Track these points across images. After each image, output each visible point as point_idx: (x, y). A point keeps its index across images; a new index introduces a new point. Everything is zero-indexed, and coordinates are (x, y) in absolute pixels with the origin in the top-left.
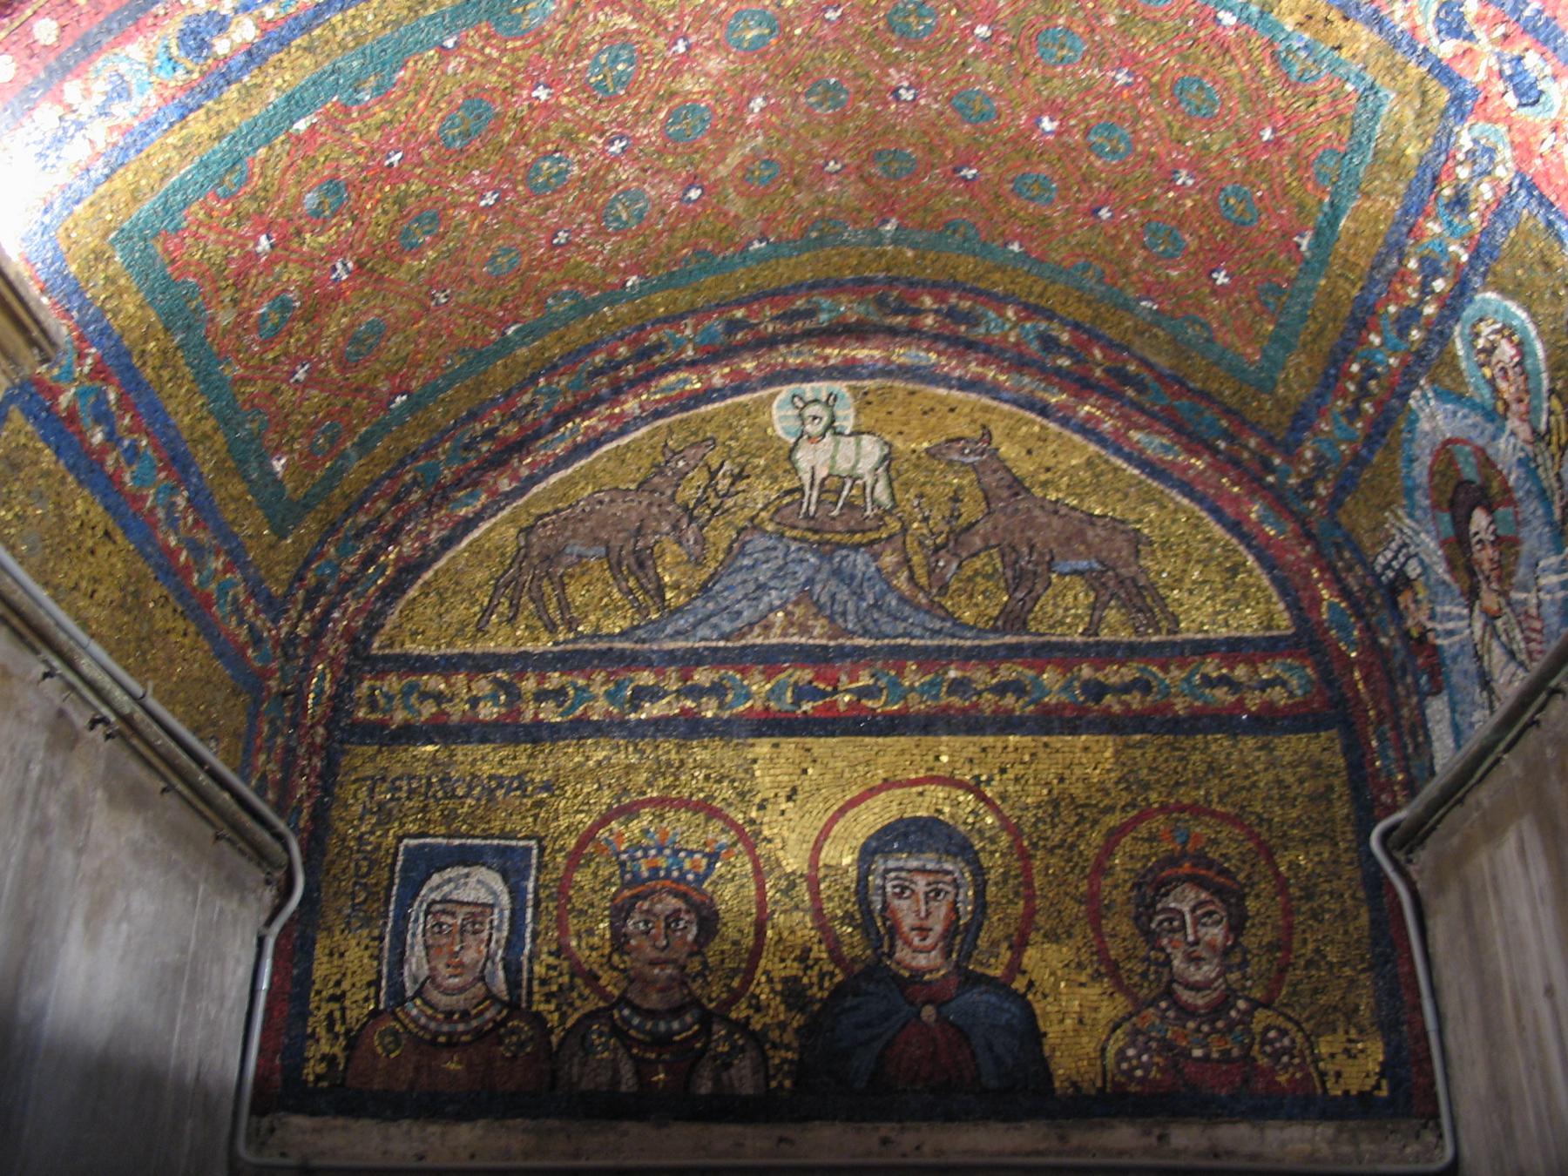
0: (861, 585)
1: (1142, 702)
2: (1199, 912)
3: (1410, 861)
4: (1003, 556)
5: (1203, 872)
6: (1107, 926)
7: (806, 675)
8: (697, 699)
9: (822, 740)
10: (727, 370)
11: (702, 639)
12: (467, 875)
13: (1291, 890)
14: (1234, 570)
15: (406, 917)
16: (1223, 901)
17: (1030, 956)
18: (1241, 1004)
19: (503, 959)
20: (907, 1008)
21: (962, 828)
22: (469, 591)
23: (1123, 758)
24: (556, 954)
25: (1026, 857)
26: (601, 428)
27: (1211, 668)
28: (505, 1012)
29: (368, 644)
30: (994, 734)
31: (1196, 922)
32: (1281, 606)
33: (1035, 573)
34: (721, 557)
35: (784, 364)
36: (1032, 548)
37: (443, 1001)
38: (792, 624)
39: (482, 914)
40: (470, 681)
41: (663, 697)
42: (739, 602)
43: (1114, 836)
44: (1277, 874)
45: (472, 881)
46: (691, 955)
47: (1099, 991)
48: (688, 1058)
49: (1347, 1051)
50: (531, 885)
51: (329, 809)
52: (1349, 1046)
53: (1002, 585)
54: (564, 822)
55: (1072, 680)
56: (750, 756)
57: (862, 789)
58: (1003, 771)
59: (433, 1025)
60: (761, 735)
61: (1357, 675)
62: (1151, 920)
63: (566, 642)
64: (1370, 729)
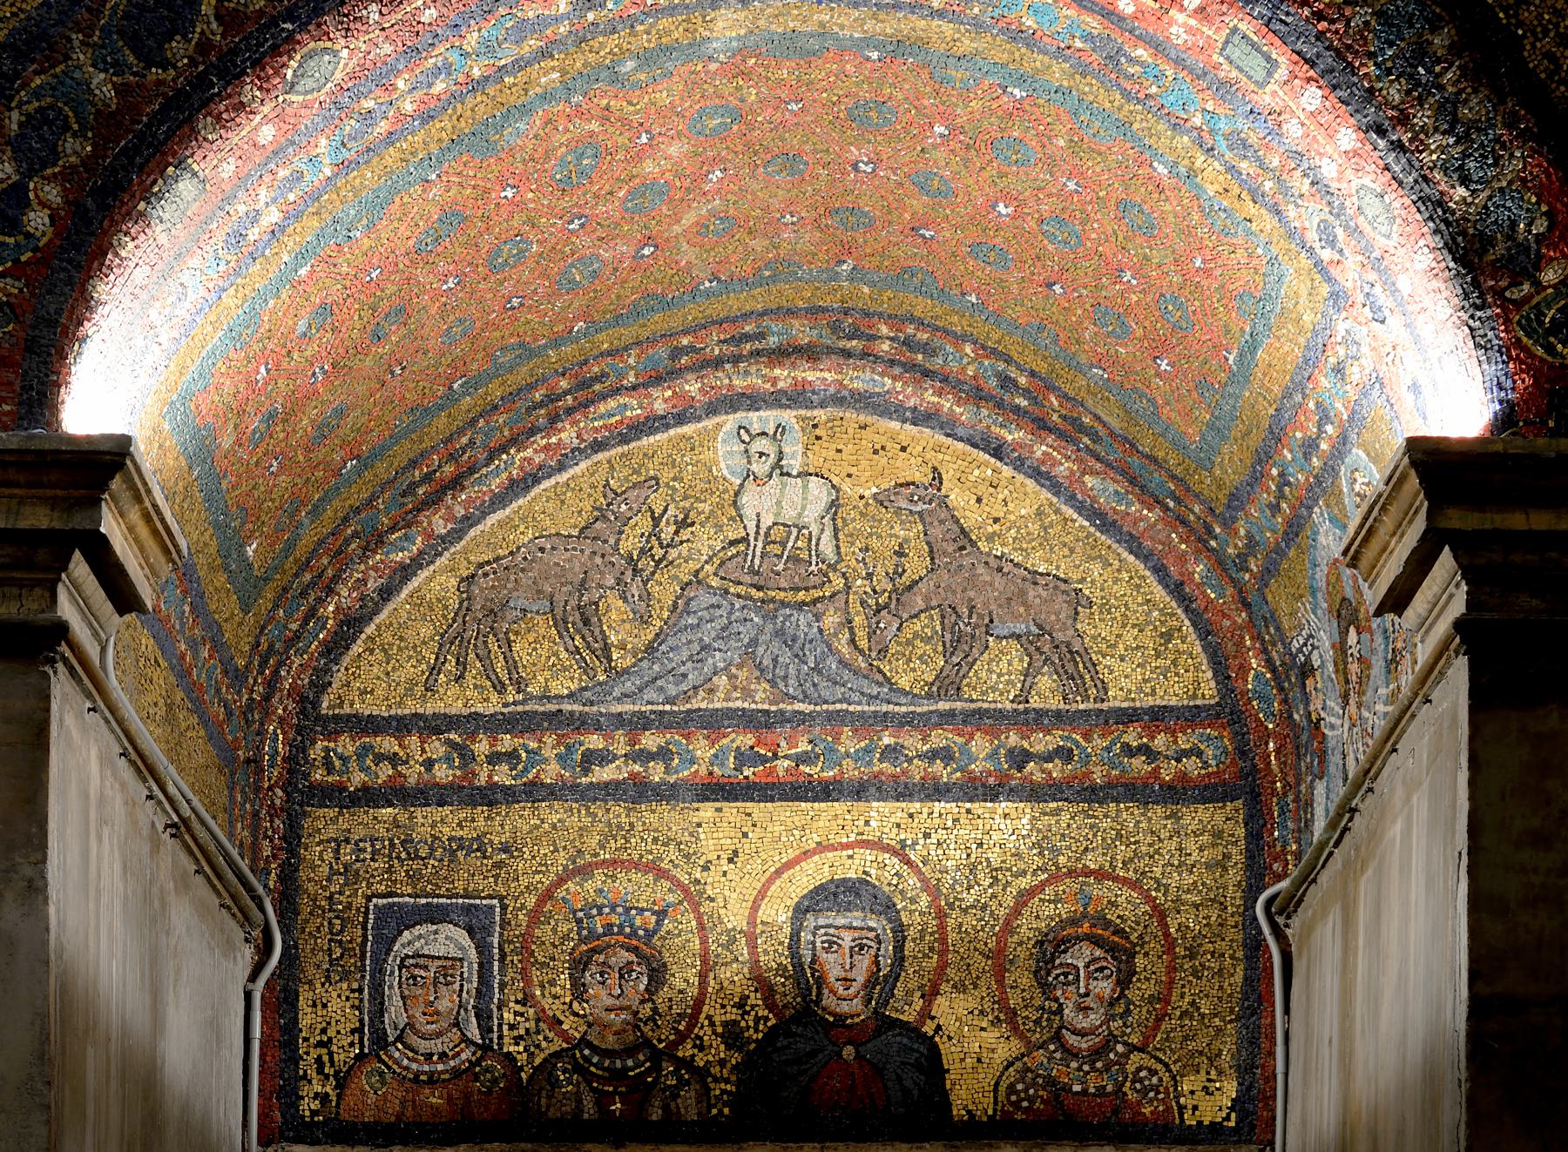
0: (802, 650)
1: (1063, 771)
2: (1092, 968)
3: (1287, 926)
4: (943, 617)
5: (1100, 932)
6: (1009, 979)
7: (746, 740)
8: (644, 763)
9: (762, 804)
10: (669, 393)
11: (649, 703)
12: (436, 932)
13: (1177, 950)
14: (1167, 637)
15: (382, 971)
16: (1114, 958)
17: (941, 1005)
18: (1120, 1048)
19: (474, 1007)
20: (830, 1047)
21: (886, 889)
22: (415, 647)
23: (1039, 825)
24: (523, 1003)
25: (941, 916)
26: (537, 461)
27: (1132, 737)
28: (479, 1053)
29: (316, 704)
30: (921, 801)
31: (1089, 977)
32: (1210, 674)
33: (973, 636)
34: (666, 614)
35: (730, 386)
36: (972, 609)
37: (423, 1046)
38: (735, 688)
39: (452, 967)
40: (422, 742)
41: (612, 762)
42: (684, 663)
43: (1025, 897)
44: (1167, 935)
45: (441, 937)
46: (643, 1002)
47: (998, 1035)
48: (639, 1092)
49: (1205, 1088)
50: (496, 941)
51: (297, 870)
52: (1207, 1084)
53: (940, 649)
54: (524, 881)
55: (998, 747)
56: (695, 820)
57: (797, 852)
58: (927, 836)
59: (414, 1066)
60: (708, 800)
61: (1271, 745)
62: (1048, 974)
63: (515, 703)
64: (1275, 799)
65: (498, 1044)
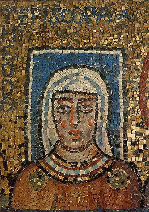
12: (77, 74)
37: (70, 156)
45: (82, 78)
50: (120, 80)
59: (64, 171)
65: (124, 156)
